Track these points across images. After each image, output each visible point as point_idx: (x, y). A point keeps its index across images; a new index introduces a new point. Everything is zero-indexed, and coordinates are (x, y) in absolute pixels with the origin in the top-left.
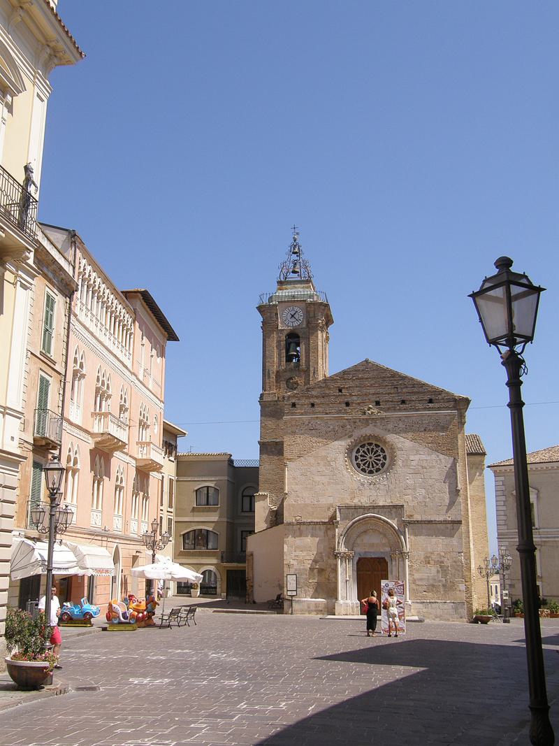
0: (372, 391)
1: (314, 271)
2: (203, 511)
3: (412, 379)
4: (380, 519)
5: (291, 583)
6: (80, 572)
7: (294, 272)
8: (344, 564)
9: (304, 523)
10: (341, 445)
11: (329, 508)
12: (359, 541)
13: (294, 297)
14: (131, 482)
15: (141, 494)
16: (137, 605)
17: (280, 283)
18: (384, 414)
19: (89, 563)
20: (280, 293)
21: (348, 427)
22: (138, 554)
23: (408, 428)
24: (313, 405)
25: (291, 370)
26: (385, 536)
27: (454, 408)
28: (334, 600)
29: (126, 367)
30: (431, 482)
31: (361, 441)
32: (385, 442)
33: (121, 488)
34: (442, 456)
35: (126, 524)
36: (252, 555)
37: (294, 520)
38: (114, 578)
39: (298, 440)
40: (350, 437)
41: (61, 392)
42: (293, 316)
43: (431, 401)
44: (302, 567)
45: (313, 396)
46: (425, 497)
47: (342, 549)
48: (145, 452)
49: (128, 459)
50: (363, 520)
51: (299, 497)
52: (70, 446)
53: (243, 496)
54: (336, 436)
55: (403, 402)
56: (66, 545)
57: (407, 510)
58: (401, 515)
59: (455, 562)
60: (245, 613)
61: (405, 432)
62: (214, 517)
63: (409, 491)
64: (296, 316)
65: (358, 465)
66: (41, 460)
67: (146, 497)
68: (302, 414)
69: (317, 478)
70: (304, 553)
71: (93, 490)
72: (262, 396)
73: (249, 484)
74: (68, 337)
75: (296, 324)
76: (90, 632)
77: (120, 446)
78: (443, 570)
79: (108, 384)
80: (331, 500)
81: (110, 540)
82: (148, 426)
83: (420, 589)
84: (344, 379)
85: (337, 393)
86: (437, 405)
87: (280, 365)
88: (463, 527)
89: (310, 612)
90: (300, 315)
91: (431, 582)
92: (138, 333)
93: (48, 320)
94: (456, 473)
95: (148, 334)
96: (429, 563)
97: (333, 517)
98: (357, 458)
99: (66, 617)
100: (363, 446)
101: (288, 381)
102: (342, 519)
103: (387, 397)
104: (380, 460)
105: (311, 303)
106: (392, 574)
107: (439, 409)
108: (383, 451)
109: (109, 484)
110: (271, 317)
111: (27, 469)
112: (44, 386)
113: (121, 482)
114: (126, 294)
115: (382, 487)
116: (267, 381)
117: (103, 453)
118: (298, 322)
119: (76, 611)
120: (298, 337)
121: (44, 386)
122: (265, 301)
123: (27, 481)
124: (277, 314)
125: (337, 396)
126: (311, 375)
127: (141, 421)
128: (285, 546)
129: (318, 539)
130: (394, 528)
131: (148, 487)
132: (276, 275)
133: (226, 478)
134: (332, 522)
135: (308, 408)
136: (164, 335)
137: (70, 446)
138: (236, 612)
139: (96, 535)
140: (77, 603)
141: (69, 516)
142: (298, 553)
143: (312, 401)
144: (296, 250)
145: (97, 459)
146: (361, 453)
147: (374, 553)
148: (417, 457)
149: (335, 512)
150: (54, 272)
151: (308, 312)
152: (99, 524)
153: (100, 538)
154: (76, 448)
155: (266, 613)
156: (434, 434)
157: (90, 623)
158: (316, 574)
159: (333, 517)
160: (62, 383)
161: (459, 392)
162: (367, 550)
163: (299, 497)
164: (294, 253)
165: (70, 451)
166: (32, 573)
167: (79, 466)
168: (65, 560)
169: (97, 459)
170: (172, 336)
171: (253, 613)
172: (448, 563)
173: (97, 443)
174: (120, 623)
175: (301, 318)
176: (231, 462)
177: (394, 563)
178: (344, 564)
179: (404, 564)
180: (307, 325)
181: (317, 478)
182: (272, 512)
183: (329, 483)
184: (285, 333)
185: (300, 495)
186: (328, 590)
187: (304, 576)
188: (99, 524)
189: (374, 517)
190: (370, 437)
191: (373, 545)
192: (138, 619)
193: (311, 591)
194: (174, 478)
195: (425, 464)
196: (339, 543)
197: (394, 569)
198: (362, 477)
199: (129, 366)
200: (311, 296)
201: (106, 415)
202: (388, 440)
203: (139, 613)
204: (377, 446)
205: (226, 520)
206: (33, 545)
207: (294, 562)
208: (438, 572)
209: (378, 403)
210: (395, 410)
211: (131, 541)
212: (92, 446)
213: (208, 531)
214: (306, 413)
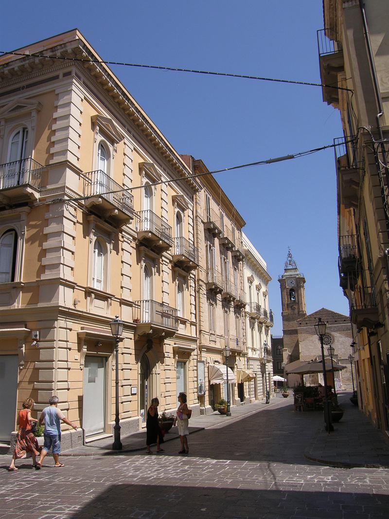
0: (326, 318)
20: (286, 274)
23: (339, 330)
24: (307, 323)
30: (346, 347)
32: (331, 335)
39: (303, 335)
43: (345, 321)
55: (336, 321)
57: (339, 356)
69: (310, 347)
72: (282, 313)
75: (293, 286)
80: (315, 354)
90: (294, 282)
107: (347, 323)
132: (283, 267)
135: (306, 325)
181: (310, 347)
182: (289, 355)
184: (289, 289)
200: (298, 275)
209: (327, 322)
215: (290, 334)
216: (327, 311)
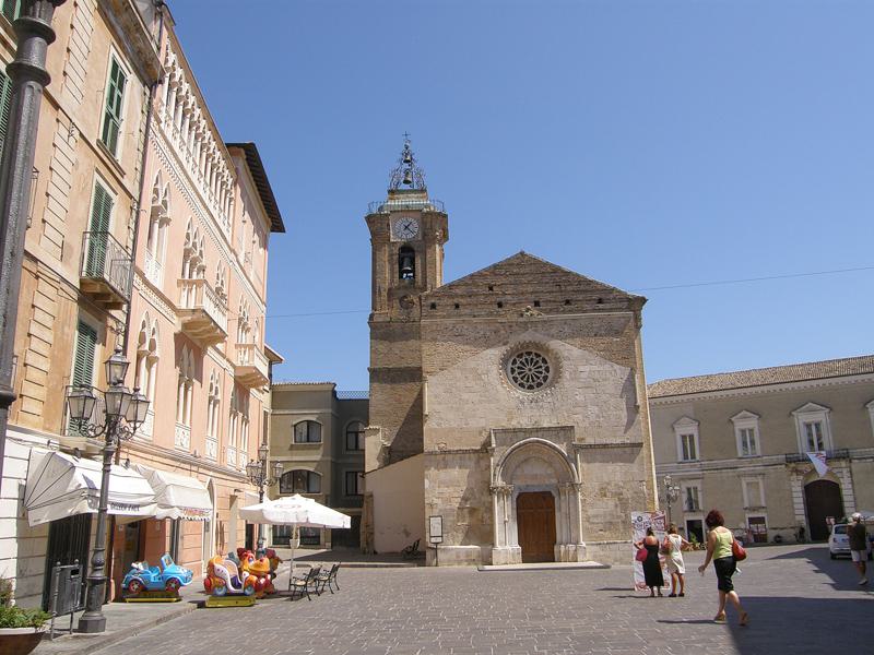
0: (530, 289)
1: (428, 182)
2: (304, 448)
3: (578, 275)
4: (546, 444)
5: (435, 526)
6: (160, 513)
7: (406, 182)
8: (502, 501)
9: (449, 452)
10: (494, 354)
11: (481, 433)
12: (519, 472)
13: (407, 206)
14: (229, 397)
15: (241, 415)
16: (256, 565)
17: (391, 192)
18: (545, 316)
19: (174, 498)
21: (503, 332)
22: (236, 494)
23: (575, 333)
24: (457, 306)
25: (406, 287)
26: (550, 464)
27: (628, 309)
28: (490, 547)
29: (225, 239)
30: (604, 397)
31: (518, 350)
32: (547, 351)
33: (216, 402)
34: (616, 367)
35: (222, 452)
36: (371, 496)
37: (437, 449)
38: (207, 525)
40: (504, 344)
41: (133, 226)
43: (600, 301)
44: (448, 507)
45: (457, 296)
46: (598, 416)
47: (499, 482)
48: (246, 358)
49: (225, 364)
50: (525, 446)
51: (442, 419)
52: (144, 318)
53: (347, 433)
54: (488, 343)
55: (568, 302)
56: (136, 469)
57: (578, 433)
58: (569, 439)
59: (636, 493)
60: (376, 566)
61: (573, 338)
62: (316, 456)
63: (578, 409)
65: (515, 379)
66: (90, 320)
67: (246, 421)
68: (444, 317)
69: (465, 396)
70: (451, 490)
71: (178, 397)
72: (371, 316)
73: (354, 419)
74: (145, 145)
75: (410, 236)
76: (179, 614)
77: (214, 335)
78: (623, 504)
79: (201, 251)
80: (482, 423)
81: (201, 470)
82: (248, 330)
83: (595, 527)
84: (496, 275)
85: (487, 291)
86: (608, 306)
88: (644, 451)
89: (460, 563)
90: (415, 227)
91: (608, 518)
92: (240, 204)
93: (114, 101)
94: (634, 385)
95: (249, 208)
96: (605, 496)
97: (487, 443)
98: (513, 371)
99: (136, 586)
100: (520, 356)
101: (401, 300)
102: (498, 445)
103: (548, 297)
104: (541, 373)
105: (428, 213)
106: (560, 510)
107: (611, 310)
108: (544, 361)
109: (199, 392)
111: (66, 329)
112: (102, 206)
113: (216, 393)
114: (229, 146)
115: (546, 405)
117: (195, 341)
119: (153, 576)
120: (413, 251)
121: (102, 206)
122: (375, 211)
123: (65, 349)
124: (388, 225)
125: (486, 296)
127: (240, 319)
128: (426, 481)
129: (467, 471)
130: (562, 454)
131: (247, 408)
132: (386, 184)
133: (330, 411)
134: (486, 449)
135: (452, 310)
136: (268, 223)
137: (144, 318)
138: (364, 566)
139: (185, 463)
140: (155, 563)
141: (141, 407)
142: (444, 489)
143: (456, 301)
144: (408, 158)
145: (185, 350)
146: (518, 364)
147: (539, 486)
148: (587, 368)
149: (490, 436)
150: (127, 29)
152: (187, 446)
153: (188, 467)
154: (151, 319)
155: (403, 566)
156: (607, 340)
157: (177, 595)
158: (467, 515)
159: (487, 443)
160: (134, 214)
161: (633, 291)
162: (529, 483)
163: (442, 419)
164: (406, 161)
165: (144, 326)
166: (70, 511)
167: (157, 353)
168: (130, 489)
169: (185, 350)
170: (277, 226)
171: (386, 566)
172: (628, 494)
173: (185, 326)
174: (229, 594)
176: (334, 393)
177: (563, 498)
178: (502, 501)
179: (576, 498)
180: (423, 237)
182: (385, 448)
183: (481, 402)
184: (399, 246)
185: (443, 416)
186: (482, 533)
187: (451, 518)
188: (187, 446)
189: (538, 441)
190: (528, 344)
191: (537, 476)
192: (257, 587)
193: (460, 536)
194: (269, 411)
195: (597, 376)
196: (495, 475)
197: (563, 505)
198: (520, 393)
199: (229, 239)
201: (199, 283)
202: (552, 347)
203: (259, 577)
204: (538, 355)
205: (329, 458)
206: (73, 461)
207: (439, 501)
208: (616, 506)
209: (537, 304)
210: (558, 312)
211: (225, 474)
212: (178, 328)
213: (309, 472)
214: (449, 316)
215: (393, 381)
216: (536, 262)
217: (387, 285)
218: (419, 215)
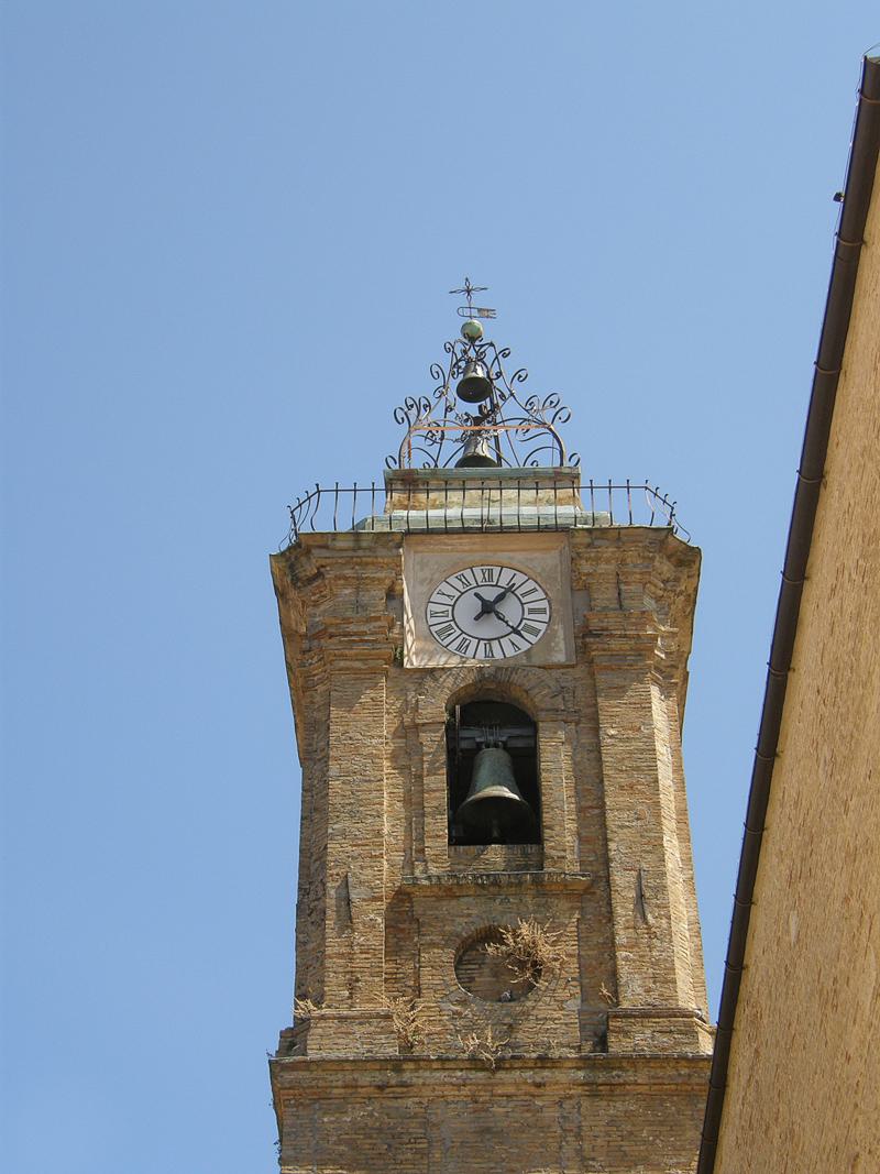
42: (488, 609)
64: (510, 609)
72: (293, 1039)
75: (507, 650)
87: (415, 852)
101: (468, 951)
110: (358, 606)
116: (334, 945)
118: (530, 632)
122: (330, 518)
124: (393, 595)
126: (623, 911)
151: (579, 585)
175: (540, 623)
217: (385, 873)
218: (549, 558)
